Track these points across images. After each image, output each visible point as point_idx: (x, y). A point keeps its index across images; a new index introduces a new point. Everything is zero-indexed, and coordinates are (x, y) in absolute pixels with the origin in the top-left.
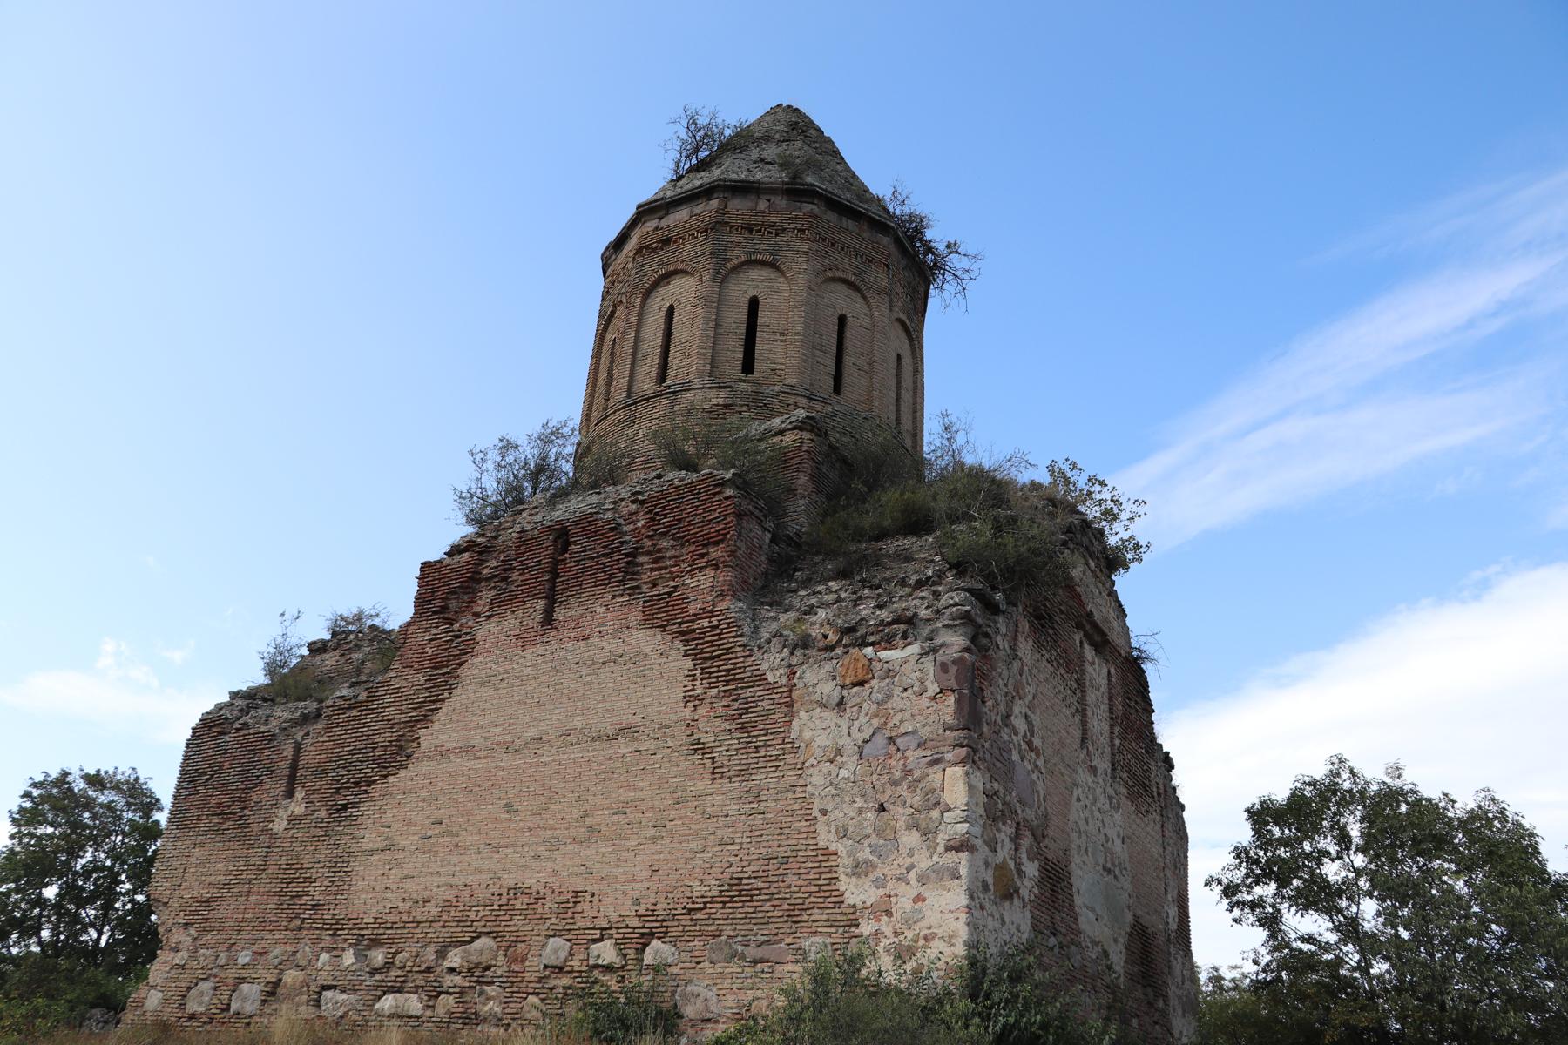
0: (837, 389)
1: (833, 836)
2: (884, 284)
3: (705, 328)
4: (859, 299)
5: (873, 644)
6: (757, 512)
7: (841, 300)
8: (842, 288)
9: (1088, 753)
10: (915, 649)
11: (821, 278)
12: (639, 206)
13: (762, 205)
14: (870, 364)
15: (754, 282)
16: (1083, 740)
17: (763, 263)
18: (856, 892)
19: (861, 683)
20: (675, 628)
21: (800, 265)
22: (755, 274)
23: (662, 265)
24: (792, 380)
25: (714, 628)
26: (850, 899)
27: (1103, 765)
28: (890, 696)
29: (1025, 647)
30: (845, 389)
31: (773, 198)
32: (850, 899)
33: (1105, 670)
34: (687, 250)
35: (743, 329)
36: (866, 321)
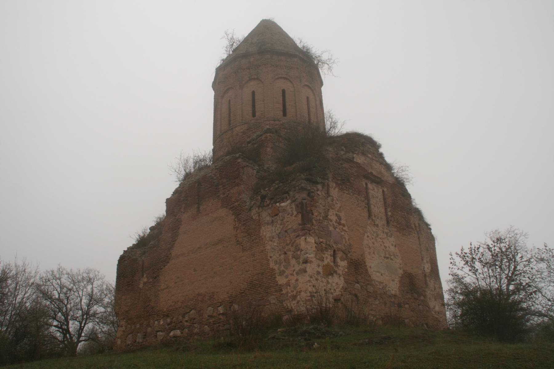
0: (285, 114)
1: (274, 264)
5: (279, 202)
6: (249, 165)
9: (373, 220)
10: (289, 202)
13: (252, 59)
16: (370, 216)
17: (254, 79)
18: (281, 280)
19: (277, 215)
20: (229, 207)
25: (239, 205)
26: (280, 283)
27: (381, 222)
28: (284, 218)
29: (334, 192)
32: (280, 283)
33: (381, 190)
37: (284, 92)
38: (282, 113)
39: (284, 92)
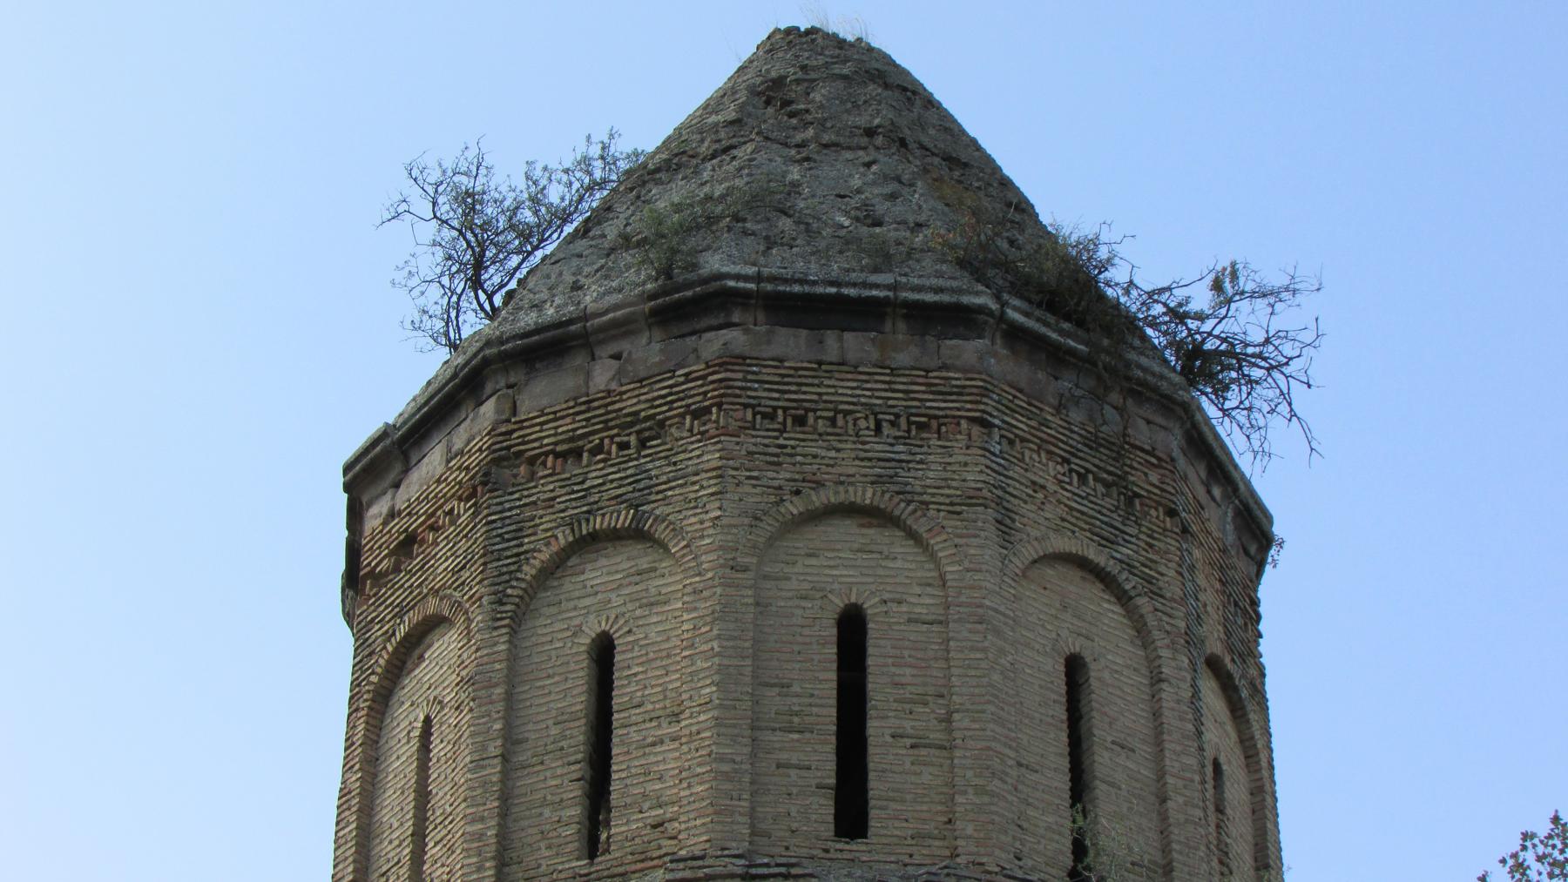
0: (852, 816)
3: (478, 764)
4: (903, 547)
7: (844, 566)
8: (844, 532)
11: (768, 526)
12: (347, 469)
13: (602, 375)
14: (948, 719)
15: (599, 593)
17: (615, 536)
22: (603, 574)
23: (400, 615)
24: (695, 842)
31: (624, 346)
34: (442, 558)
35: (577, 736)
36: (925, 603)
37: (852, 629)
38: (823, 809)
39: (852, 629)
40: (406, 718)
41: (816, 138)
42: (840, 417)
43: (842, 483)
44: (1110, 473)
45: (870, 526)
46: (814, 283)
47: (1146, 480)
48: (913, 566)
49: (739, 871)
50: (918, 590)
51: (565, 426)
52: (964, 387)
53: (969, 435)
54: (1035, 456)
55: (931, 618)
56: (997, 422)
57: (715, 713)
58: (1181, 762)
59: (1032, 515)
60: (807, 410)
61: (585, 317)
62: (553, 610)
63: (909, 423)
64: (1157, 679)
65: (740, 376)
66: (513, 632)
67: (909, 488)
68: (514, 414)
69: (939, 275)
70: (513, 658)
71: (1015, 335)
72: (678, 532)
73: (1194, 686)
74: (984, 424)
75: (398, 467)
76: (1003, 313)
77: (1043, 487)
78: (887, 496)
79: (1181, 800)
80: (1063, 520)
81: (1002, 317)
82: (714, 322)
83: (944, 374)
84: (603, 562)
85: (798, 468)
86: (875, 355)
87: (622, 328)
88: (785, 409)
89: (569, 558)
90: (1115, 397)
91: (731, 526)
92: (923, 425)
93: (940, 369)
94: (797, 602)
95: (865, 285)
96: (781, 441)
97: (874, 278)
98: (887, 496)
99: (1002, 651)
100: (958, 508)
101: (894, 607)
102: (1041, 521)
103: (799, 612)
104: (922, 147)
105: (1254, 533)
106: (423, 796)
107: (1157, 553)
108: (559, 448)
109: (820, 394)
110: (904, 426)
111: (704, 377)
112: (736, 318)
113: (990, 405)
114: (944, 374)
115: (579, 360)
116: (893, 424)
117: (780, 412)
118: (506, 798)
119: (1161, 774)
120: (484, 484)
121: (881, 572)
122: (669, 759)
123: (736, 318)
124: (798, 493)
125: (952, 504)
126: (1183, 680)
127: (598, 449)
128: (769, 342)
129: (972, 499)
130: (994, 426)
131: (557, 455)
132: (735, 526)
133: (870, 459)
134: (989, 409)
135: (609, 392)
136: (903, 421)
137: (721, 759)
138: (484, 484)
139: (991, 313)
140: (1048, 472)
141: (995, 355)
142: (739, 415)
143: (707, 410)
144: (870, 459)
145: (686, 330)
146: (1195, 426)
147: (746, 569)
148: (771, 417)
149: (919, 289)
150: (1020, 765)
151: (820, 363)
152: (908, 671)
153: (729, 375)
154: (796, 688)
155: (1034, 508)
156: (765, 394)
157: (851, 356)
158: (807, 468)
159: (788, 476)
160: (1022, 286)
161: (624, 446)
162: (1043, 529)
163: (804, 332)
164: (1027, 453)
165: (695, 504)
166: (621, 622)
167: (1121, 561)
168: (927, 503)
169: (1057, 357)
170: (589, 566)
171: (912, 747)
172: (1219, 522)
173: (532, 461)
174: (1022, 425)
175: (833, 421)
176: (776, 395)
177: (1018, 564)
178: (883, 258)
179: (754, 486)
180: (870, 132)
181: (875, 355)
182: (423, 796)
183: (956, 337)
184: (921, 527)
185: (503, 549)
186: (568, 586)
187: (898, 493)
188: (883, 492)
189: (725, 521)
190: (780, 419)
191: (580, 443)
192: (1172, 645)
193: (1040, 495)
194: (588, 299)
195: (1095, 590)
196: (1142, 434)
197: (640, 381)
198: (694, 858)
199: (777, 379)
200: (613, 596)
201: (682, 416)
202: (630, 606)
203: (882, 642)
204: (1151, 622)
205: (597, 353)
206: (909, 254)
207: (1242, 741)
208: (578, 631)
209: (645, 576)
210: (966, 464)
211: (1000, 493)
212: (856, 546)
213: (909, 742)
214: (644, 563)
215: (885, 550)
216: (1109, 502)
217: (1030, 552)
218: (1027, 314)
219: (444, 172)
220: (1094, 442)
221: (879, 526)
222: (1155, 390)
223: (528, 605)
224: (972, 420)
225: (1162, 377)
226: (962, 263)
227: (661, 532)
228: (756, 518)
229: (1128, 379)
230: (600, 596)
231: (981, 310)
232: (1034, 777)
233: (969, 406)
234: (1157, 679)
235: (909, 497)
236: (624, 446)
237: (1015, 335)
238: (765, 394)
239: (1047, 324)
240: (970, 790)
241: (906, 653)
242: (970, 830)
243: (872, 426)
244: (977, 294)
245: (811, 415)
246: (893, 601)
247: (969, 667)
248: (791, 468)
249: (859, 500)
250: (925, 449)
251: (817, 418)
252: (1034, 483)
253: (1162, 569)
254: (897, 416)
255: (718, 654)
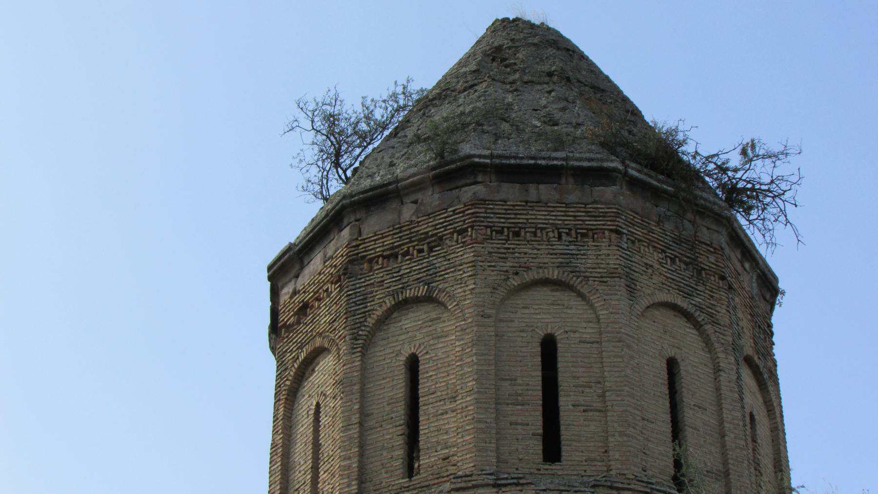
0: (552, 451)
2: (613, 262)
3: (346, 428)
7: (544, 313)
8: (544, 294)
11: (502, 292)
12: (270, 268)
13: (407, 212)
14: (603, 396)
15: (410, 332)
17: (417, 301)
21: (465, 280)
23: (301, 347)
24: (466, 466)
30: (566, 451)
31: (419, 196)
34: (324, 316)
35: (400, 411)
37: (549, 348)
38: (536, 447)
39: (549, 348)
40: (306, 404)
41: (520, 79)
42: (538, 231)
43: (541, 267)
44: (688, 257)
45: (557, 290)
46: (522, 158)
47: (708, 260)
48: (581, 312)
49: (491, 482)
50: (584, 325)
51: (388, 241)
52: (606, 212)
53: (610, 239)
54: (647, 249)
55: (592, 340)
56: (625, 231)
57: (475, 396)
58: (732, 415)
59: (645, 282)
60: (520, 228)
61: (397, 181)
62: (385, 342)
63: (577, 233)
64: (717, 370)
65: (483, 210)
66: (363, 355)
67: (577, 269)
68: (360, 234)
69: (590, 151)
70: (364, 369)
71: (633, 183)
72: (451, 297)
73: (738, 372)
74: (618, 232)
75: (297, 267)
76: (626, 172)
77: (652, 266)
78: (566, 274)
79: (732, 436)
80: (663, 284)
81: (626, 174)
82: (468, 181)
83: (595, 206)
84: (411, 315)
85: (516, 260)
86: (557, 197)
87: (417, 186)
88: (508, 228)
89: (392, 313)
90: (689, 216)
91: (480, 293)
92: (585, 234)
93: (592, 203)
94: (518, 334)
95: (550, 158)
96: (507, 246)
97: (555, 155)
98: (566, 274)
99: (632, 357)
100: (605, 279)
101: (572, 335)
102: (651, 285)
103: (520, 339)
104: (579, 81)
105: (768, 288)
106: (316, 446)
107: (715, 300)
108: (385, 254)
109: (527, 219)
110: (574, 235)
111: (463, 212)
112: (480, 179)
113: (621, 222)
114: (595, 206)
115: (395, 204)
116: (568, 234)
117: (506, 230)
118: (362, 446)
119: (721, 422)
120: (345, 274)
121: (563, 315)
122: (451, 422)
123: (480, 179)
124: (517, 274)
125: (602, 277)
126: (732, 370)
127: (407, 253)
128: (498, 192)
129: (612, 274)
130: (624, 233)
131: (384, 257)
132: (483, 293)
133: (556, 254)
134: (620, 224)
135: (412, 222)
136: (573, 232)
137: (479, 421)
138: (345, 274)
139: (619, 171)
140: (653, 257)
141: (622, 194)
142: (484, 231)
143: (466, 230)
144: (556, 254)
145: (453, 186)
146: (734, 230)
147: (489, 317)
148: (501, 232)
149: (580, 159)
150: (643, 419)
151: (527, 202)
152: (581, 370)
153: (477, 210)
154: (519, 381)
155: (646, 278)
156: (497, 220)
157: (544, 198)
158: (521, 260)
159: (511, 264)
160: (637, 156)
161: (421, 251)
162: (652, 289)
163: (518, 185)
164: (642, 247)
165: (461, 282)
166: (422, 347)
167: (695, 305)
168: (588, 277)
169: (657, 194)
170: (403, 318)
171: (584, 411)
172: (749, 282)
173: (370, 261)
174: (638, 232)
175: (535, 234)
176: (503, 220)
177: (639, 309)
178: (559, 143)
179: (493, 271)
180: (550, 74)
181: (557, 197)
182: (316, 446)
183: (601, 185)
184: (585, 290)
185: (356, 309)
186: (392, 329)
187: (572, 272)
188: (564, 272)
189: (477, 290)
190: (506, 233)
191: (397, 250)
192: (725, 351)
193: (650, 271)
194: (399, 171)
195: (682, 322)
196: (705, 235)
197: (429, 215)
198: (467, 476)
199: (503, 211)
200: (417, 333)
201: (452, 233)
202: (427, 339)
203: (566, 354)
204: (713, 338)
205: (404, 200)
206: (574, 140)
207: (765, 402)
208: (399, 353)
209: (435, 322)
210: (608, 255)
211: (628, 270)
212: (549, 302)
213: (582, 408)
214: (434, 315)
215: (566, 303)
216: (688, 273)
217: (645, 302)
218: (639, 171)
219: (317, 104)
220: (678, 240)
221: (562, 290)
222: (711, 211)
223: (371, 340)
224: (611, 230)
225: (715, 203)
226: (603, 145)
227: (442, 297)
228: (494, 288)
229: (697, 205)
230: (410, 334)
231: (615, 170)
232: (652, 425)
233: (609, 223)
234: (717, 370)
235: (578, 274)
236: (421, 251)
237: (633, 183)
238: (497, 220)
239: (650, 176)
240: (617, 434)
241: (579, 360)
242: (617, 456)
243: (557, 236)
244: (612, 161)
245: (523, 230)
246: (571, 331)
247: (614, 366)
248: (513, 260)
249: (550, 277)
250: (586, 248)
251: (526, 232)
252: (646, 264)
253: (718, 309)
254: (570, 230)
255: (476, 363)
